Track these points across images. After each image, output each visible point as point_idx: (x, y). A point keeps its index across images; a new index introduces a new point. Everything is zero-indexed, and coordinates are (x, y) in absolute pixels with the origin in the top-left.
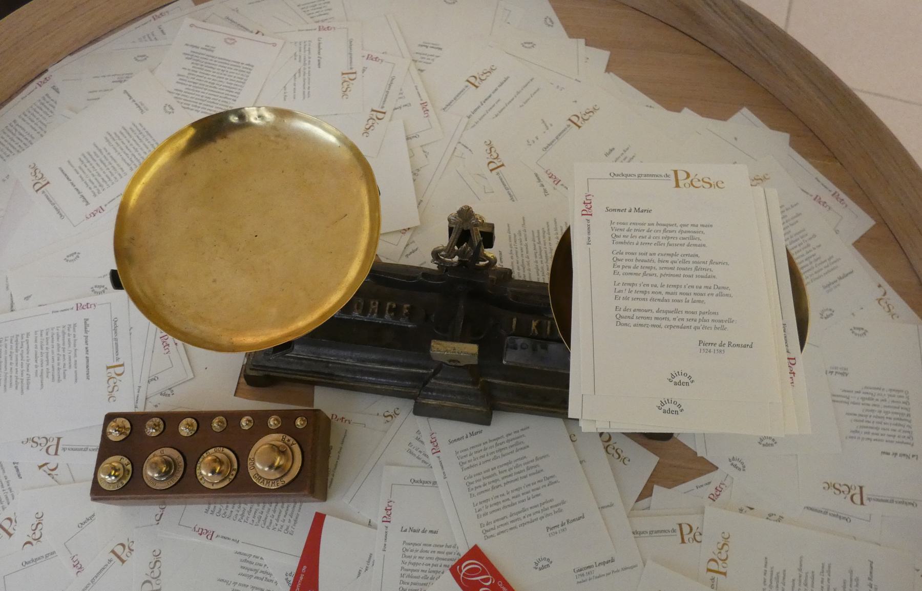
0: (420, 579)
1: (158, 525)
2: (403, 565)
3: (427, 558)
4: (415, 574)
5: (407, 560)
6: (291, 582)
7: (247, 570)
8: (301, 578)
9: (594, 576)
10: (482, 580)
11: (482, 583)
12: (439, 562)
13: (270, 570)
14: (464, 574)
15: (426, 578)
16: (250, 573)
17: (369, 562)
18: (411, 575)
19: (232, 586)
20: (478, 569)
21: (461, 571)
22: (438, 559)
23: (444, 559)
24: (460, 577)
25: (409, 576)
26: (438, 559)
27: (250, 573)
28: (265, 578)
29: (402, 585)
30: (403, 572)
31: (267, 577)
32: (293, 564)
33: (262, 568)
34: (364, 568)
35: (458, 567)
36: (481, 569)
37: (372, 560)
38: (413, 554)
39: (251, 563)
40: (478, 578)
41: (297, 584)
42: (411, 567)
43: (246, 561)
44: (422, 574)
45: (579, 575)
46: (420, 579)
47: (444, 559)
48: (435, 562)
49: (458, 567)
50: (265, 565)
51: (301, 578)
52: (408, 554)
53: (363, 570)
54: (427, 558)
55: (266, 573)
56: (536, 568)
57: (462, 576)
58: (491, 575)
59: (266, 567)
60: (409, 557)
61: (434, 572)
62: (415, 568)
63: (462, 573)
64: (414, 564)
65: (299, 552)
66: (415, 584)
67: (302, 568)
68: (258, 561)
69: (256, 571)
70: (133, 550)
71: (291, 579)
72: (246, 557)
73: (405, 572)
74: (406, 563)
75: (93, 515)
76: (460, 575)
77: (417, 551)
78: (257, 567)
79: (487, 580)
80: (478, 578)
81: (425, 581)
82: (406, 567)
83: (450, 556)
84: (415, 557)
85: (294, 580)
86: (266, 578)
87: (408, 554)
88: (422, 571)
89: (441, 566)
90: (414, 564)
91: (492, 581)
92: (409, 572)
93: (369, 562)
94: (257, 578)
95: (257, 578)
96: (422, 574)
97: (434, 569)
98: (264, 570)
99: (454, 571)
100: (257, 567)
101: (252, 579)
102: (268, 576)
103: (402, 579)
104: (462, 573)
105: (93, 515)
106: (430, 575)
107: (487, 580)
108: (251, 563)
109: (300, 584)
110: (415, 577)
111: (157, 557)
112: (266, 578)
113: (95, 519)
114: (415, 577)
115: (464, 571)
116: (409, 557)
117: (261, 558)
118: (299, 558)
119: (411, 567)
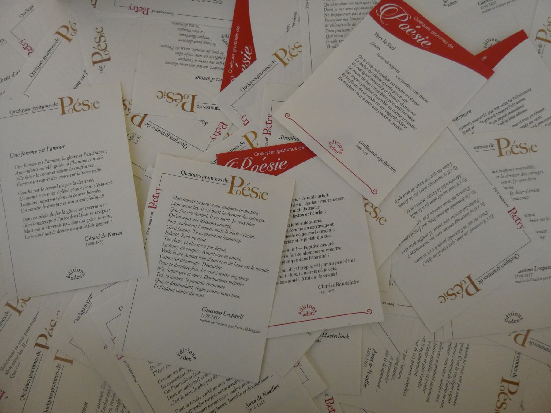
0: (343, 26)
1: (95, 8)
2: (326, 17)
3: (347, 9)
4: (338, 23)
5: (329, 13)
6: (228, 42)
7: (186, 37)
8: (237, 37)
9: (496, 6)
10: (399, 18)
11: (400, 20)
12: (358, 11)
13: (206, 35)
14: (383, 16)
15: (348, 25)
17: (294, 19)
18: (334, 24)
19: (175, 50)
20: (395, 10)
21: (380, 13)
22: (357, 8)
23: (362, 9)
24: (380, 18)
25: (333, 25)
26: (357, 8)
28: (203, 42)
29: (328, 33)
30: (327, 23)
31: (206, 40)
32: (226, 27)
33: (199, 34)
34: (292, 25)
35: (377, 11)
36: (397, 9)
37: (297, 17)
38: (333, 7)
39: (188, 31)
40: (397, 17)
41: (234, 38)
42: (334, 18)
43: (183, 29)
44: (345, 22)
45: (483, 6)
46: (343, 26)
47: (362, 9)
48: (354, 11)
49: (377, 11)
50: (202, 32)
51: (237, 37)
52: (328, 7)
53: (291, 26)
54: (347, 9)
55: (204, 37)
56: (445, 5)
57: (381, 17)
58: (407, 13)
59: (203, 33)
60: (331, 10)
61: (355, 19)
62: (337, 18)
63: (381, 15)
64: (336, 15)
65: (231, 16)
66: (339, 31)
67: (236, 28)
68: (195, 28)
70: (76, 30)
71: (227, 39)
72: (183, 27)
73: (329, 23)
74: (329, 15)
75: (32, 7)
76: (380, 17)
77: (337, 4)
78: (195, 34)
79: (404, 17)
80: (397, 17)
82: (329, 18)
83: (366, 6)
84: (336, 10)
86: (205, 42)
87: (328, 7)
88: (344, 20)
89: (360, 14)
90: (336, 15)
91: (409, 17)
92: (333, 22)
93: (294, 19)
94: (197, 42)
95: (197, 42)
96: (345, 22)
97: (354, 17)
98: (201, 35)
99: (374, 14)
100: (195, 34)
101: (192, 43)
102: (206, 40)
103: (327, 28)
104: (381, 15)
105: (32, 7)
106: (352, 22)
107: (404, 17)
108: (188, 31)
110: (339, 26)
111: (101, 34)
112: (205, 42)
113: (34, 9)
114: (339, 26)
115: (382, 13)
116: (331, 10)
117: (197, 26)
118: (232, 21)
119: (334, 18)
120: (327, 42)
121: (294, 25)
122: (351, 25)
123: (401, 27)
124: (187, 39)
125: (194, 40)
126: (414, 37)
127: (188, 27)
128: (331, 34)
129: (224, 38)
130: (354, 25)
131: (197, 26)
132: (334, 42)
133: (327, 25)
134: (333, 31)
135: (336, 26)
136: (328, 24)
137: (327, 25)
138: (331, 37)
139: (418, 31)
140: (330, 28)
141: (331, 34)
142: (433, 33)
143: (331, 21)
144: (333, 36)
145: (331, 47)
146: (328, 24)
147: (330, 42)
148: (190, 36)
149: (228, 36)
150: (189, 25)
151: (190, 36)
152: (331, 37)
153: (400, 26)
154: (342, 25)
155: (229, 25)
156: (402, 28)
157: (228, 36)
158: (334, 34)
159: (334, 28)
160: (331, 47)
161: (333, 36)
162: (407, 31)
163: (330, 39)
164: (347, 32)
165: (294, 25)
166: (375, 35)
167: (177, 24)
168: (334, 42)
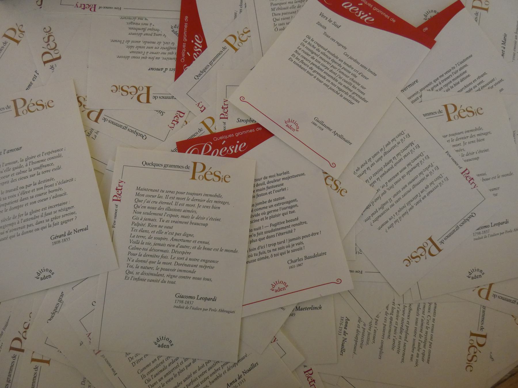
6: (178, 32)
8: (186, 26)
13: (156, 27)
15: (293, 7)
16: (139, 32)
17: (241, 5)
18: (280, 7)
19: (125, 44)
25: (279, 9)
27: (139, 32)
28: (153, 34)
29: (275, 17)
30: (273, 7)
31: (156, 32)
34: (239, 11)
37: (243, 4)
39: (137, 24)
43: (131, 23)
50: (151, 24)
51: (186, 26)
53: (238, 13)
59: (152, 25)
66: (285, 14)
68: (144, 21)
69: (144, 29)
70: (24, 32)
71: (177, 30)
72: (132, 21)
73: (275, 6)
78: (144, 27)
81: (293, 10)
85: (179, 30)
86: (155, 34)
92: (278, 6)
93: (241, 5)
94: (147, 34)
95: (147, 34)
100: (144, 27)
101: (142, 36)
102: (156, 32)
103: (273, 12)
108: (137, 24)
109: (186, 31)
110: (285, 9)
112: (155, 34)
114: (285, 9)
117: (146, 19)
120: (275, 25)
121: (241, 12)
122: (296, 8)
123: (344, 6)
124: (137, 32)
125: (144, 33)
126: (358, 14)
127: (136, 21)
128: (277, 17)
129: (174, 29)
130: (299, 7)
131: (146, 19)
132: (281, 25)
133: (273, 9)
134: (280, 14)
135: (281, 9)
136: (274, 8)
137: (273, 9)
138: (278, 20)
139: (361, 8)
140: (276, 12)
141: (277, 17)
142: (375, 9)
143: (276, 5)
144: (280, 19)
145: (279, 30)
146: (274, 8)
147: (278, 25)
148: (139, 29)
149: (177, 27)
150: (137, 18)
151: (139, 29)
152: (278, 20)
153: (343, 5)
154: (287, 8)
155: (178, 15)
156: (345, 7)
157: (177, 27)
158: (281, 17)
159: (280, 12)
160: (279, 30)
161: (280, 19)
162: (350, 9)
163: (277, 23)
164: (293, 15)
165: (241, 12)
166: (320, 15)
167: (125, 18)
168: (281, 25)
